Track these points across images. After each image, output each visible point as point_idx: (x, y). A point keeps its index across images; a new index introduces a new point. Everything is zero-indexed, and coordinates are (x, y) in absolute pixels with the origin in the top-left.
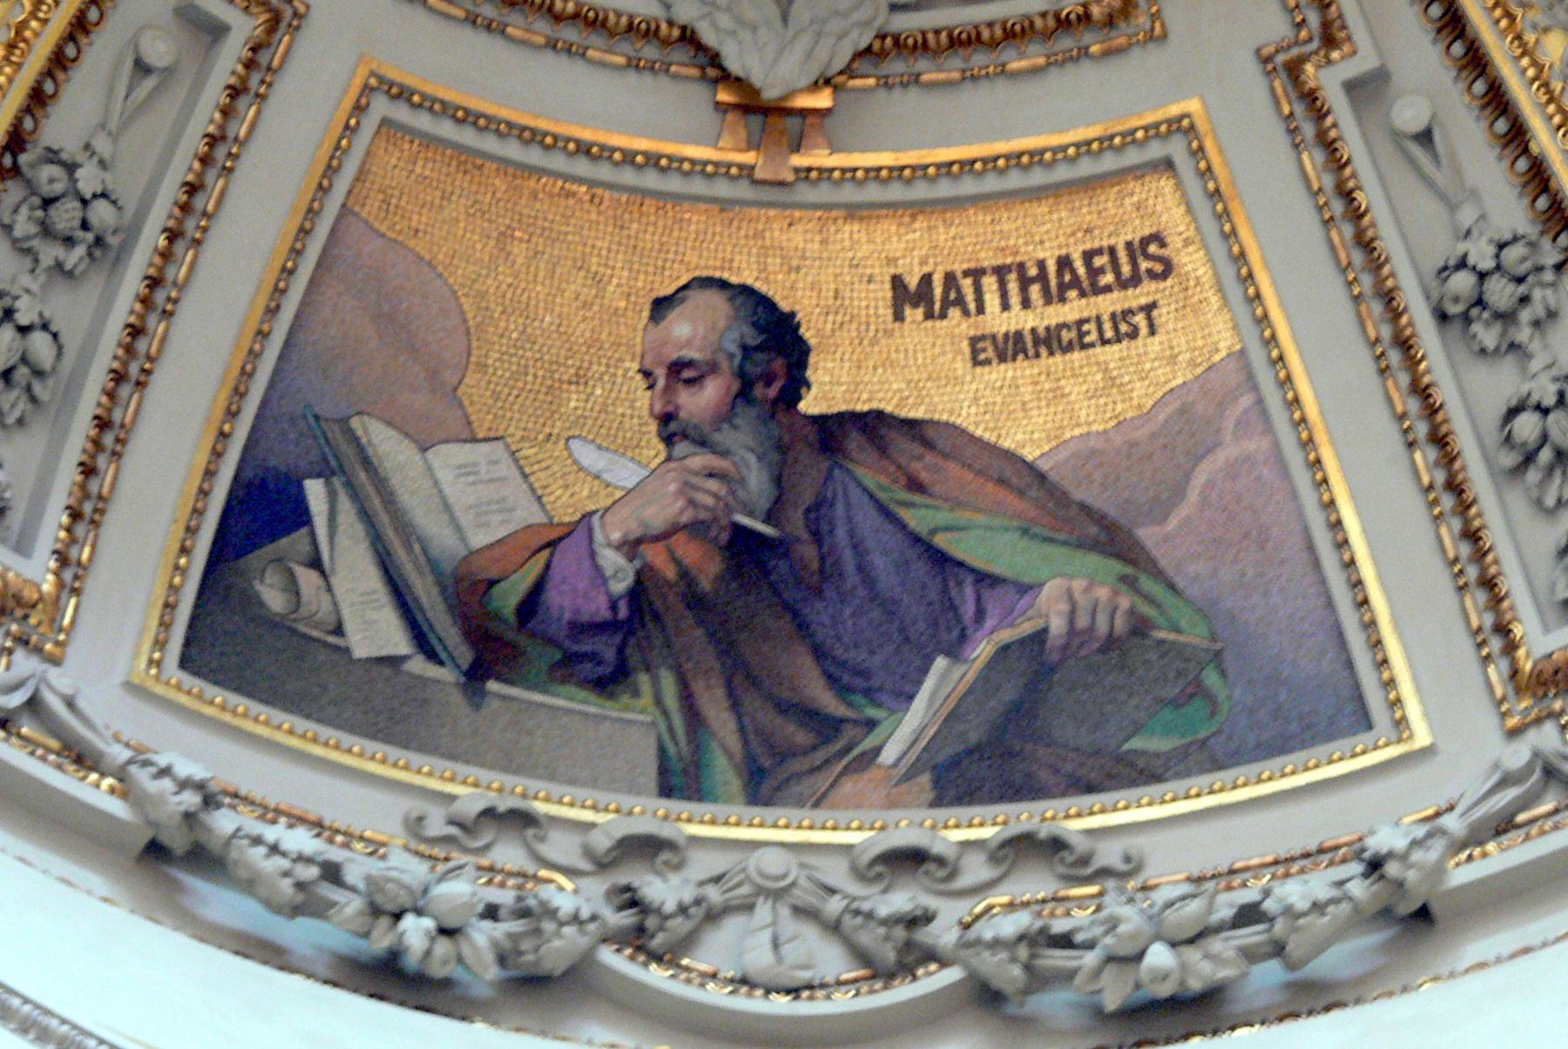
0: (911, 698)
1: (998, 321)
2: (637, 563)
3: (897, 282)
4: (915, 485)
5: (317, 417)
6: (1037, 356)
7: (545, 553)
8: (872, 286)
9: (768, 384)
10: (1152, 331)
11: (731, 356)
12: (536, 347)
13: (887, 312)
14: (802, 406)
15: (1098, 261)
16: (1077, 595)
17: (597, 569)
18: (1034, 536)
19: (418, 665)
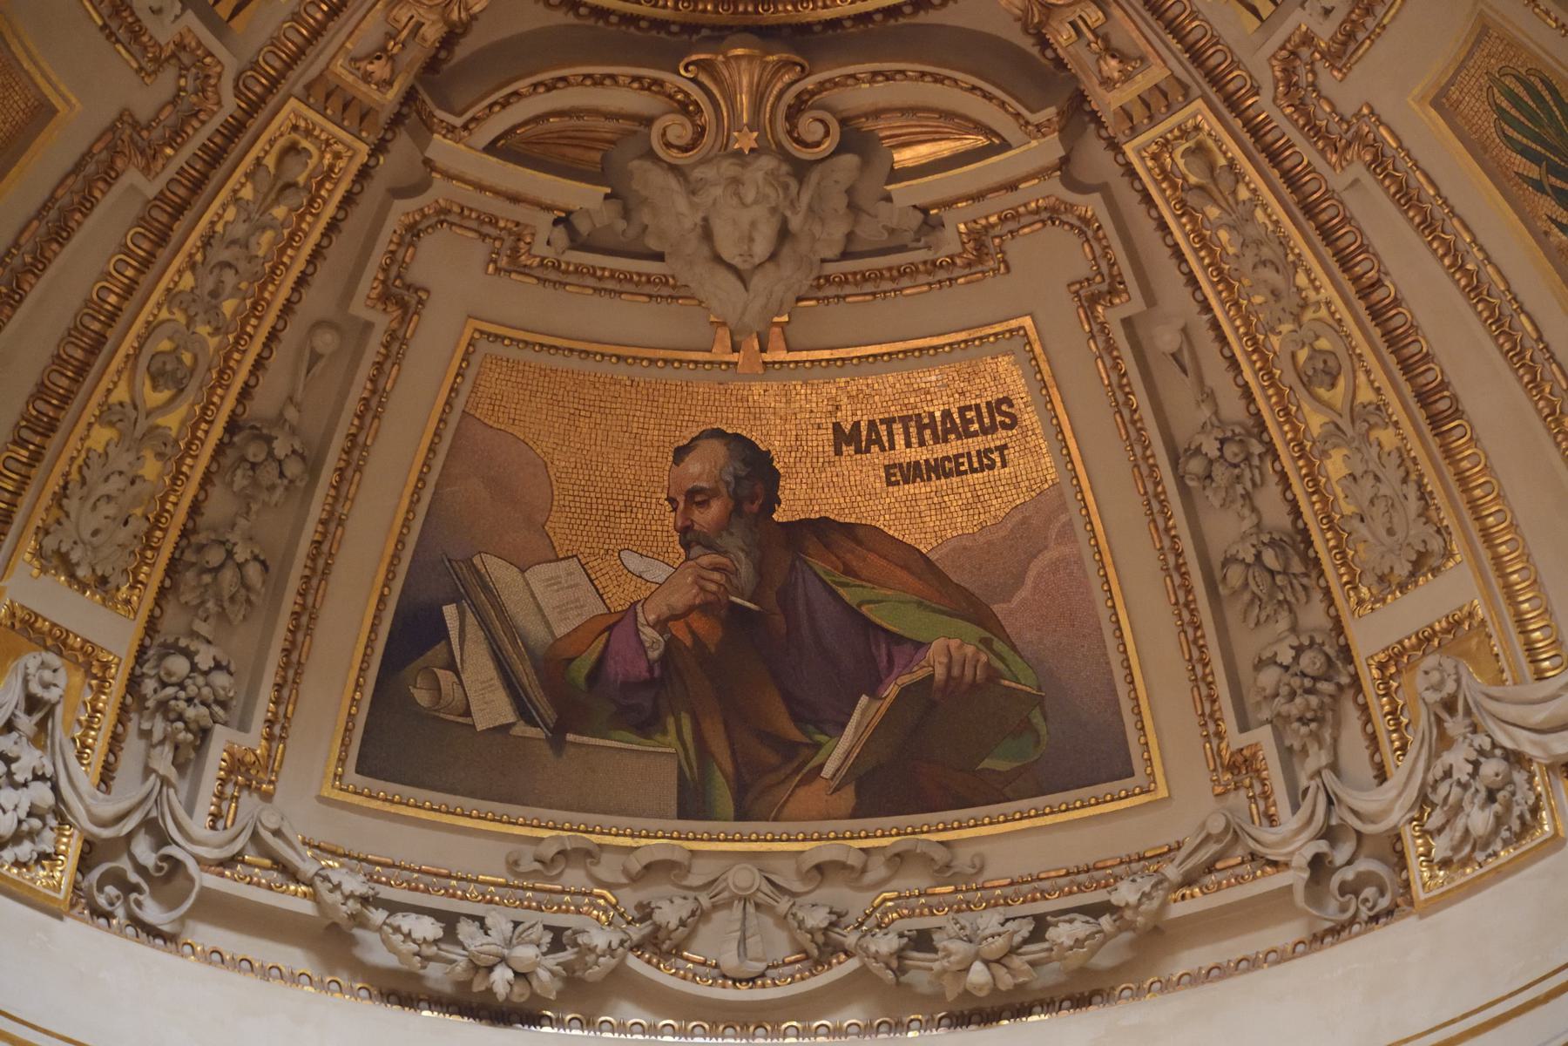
0: (844, 726)
1: (904, 454)
2: (666, 636)
3: (837, 427)
4: (848, 571)
5: (449, 561)
6: (929, 479)
7: (606, 634)
8: (820, 432)
9: (753, 503)
10: (1004, 465)
11: (728, 484)
12: (598, 490)
13: (830, 450)
14: (775, 516)
15: (970, 415)
16: (952, 650)
17: (641, 642)
18: (927, 607)
19: (522, 730)
